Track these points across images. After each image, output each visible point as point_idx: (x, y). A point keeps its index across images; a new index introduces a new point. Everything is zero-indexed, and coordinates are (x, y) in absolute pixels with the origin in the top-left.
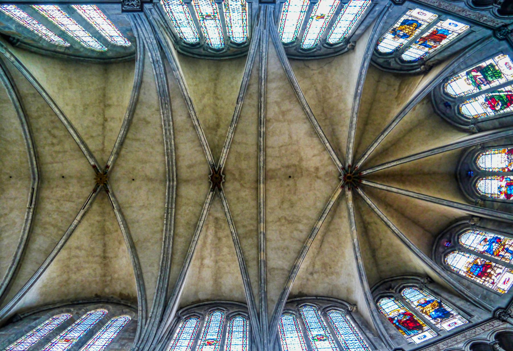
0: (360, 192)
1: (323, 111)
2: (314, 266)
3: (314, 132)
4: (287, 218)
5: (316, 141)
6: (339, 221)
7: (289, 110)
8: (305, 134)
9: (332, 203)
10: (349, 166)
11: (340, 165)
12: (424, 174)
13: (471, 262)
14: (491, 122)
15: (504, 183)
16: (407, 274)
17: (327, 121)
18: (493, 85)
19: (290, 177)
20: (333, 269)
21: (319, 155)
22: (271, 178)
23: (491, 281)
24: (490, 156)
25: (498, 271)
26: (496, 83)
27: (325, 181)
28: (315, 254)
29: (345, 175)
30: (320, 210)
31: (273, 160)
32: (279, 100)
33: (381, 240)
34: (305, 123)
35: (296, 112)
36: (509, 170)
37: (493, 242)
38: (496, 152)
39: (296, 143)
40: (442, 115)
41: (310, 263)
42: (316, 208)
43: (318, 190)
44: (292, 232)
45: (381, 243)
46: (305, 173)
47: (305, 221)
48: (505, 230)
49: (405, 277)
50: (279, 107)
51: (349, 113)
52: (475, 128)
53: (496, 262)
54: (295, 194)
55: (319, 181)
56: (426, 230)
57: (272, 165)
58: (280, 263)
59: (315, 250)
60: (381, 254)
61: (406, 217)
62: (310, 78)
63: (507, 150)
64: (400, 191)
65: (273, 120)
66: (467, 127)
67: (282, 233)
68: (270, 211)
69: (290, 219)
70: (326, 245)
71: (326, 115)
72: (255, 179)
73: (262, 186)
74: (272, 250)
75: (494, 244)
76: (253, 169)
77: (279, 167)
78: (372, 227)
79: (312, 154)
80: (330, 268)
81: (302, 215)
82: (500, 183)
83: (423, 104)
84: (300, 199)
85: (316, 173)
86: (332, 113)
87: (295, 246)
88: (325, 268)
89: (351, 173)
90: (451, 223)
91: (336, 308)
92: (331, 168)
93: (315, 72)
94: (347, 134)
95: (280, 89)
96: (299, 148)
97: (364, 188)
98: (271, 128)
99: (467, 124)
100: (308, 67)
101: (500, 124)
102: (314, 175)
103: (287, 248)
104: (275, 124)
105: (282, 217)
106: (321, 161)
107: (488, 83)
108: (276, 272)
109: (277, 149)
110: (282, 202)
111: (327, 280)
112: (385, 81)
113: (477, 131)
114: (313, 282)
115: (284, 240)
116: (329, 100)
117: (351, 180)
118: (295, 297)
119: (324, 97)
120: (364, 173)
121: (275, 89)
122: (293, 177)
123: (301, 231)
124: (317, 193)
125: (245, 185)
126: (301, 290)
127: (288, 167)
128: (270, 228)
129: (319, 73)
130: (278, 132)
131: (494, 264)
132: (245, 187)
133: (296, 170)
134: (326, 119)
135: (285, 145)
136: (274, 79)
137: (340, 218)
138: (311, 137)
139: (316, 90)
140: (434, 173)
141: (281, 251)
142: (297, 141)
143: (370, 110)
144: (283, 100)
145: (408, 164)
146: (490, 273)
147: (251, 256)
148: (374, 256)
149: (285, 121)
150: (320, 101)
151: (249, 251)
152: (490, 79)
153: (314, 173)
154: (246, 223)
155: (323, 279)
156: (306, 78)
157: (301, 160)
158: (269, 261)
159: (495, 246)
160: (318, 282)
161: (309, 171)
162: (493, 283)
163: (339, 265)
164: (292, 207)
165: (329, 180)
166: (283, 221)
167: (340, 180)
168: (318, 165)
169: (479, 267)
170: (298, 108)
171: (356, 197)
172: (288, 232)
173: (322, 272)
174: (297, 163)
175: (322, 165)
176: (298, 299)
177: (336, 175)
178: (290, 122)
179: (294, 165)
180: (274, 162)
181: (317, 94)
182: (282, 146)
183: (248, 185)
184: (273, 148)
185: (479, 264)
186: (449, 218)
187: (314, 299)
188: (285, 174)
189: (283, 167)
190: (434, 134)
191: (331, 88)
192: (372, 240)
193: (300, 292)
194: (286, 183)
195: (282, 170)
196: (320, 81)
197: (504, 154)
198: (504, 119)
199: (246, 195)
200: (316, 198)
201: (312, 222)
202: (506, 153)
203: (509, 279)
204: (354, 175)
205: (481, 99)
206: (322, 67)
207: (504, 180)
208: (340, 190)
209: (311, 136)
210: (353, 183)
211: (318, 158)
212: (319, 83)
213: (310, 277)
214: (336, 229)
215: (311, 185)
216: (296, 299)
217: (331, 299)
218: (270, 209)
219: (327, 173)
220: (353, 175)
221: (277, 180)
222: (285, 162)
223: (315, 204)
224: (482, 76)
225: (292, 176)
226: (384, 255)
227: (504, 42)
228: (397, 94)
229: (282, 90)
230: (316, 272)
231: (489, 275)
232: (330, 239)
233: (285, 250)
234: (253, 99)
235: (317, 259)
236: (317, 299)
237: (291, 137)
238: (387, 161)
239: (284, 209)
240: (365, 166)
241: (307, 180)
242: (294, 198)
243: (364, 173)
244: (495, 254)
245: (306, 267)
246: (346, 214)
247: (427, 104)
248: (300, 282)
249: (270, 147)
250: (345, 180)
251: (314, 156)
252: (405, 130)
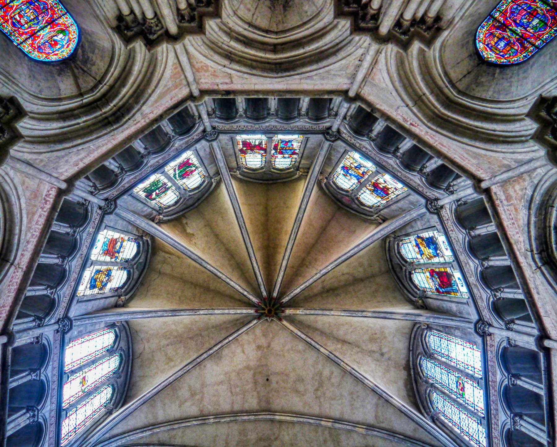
0: (285, 300)
1: (191, 338)
2: (374, 352)
3: (216, 356)
4: (315, 388)
5: (226, 352)
6: (320, 323)
7: (190, 387)
8: (217, 365)
9: (299, 333)
10: (256, 311)
11: (255, 322)
12: (267, 220)
16: (384, 245)
17: (203, 333)
19: (267, 380)
20: (377, 332)
21: (242, 346)
22: (268, 402)
27: (273, 338)
28: (359, 350)
29: (266, 316)
30: (307, 347)
31: (246, 401)
32: (177, 403)
33: (343, 274)
34: (205, 366)
35: (192, 380)
39: (228, 375)
40: (200, 202)
41: (369, 356)
42: (304, 351)
43: (284, 347)
44: (333, 385)
45: (347, 274)
46: (264, 362)
47: (320, 366)
49: (387, 249)
50: (186, 401)
51: (196, 318)
52: (216, 178)
54: (287, 375)
55: (273, 345)
56: (332, 219)
57: (253, 403)
58: (369, 407)
59: (354, 350)
60: (360, 273)
61: (316, 242)
62: (153, 352)
64: (286, 257)
65: (201, 406)
67: (333, 397)
68: (307, 408)
69: (316, 384)
70: (348, 338)
71: (197, 335)
72: (270, 422)
73: (277, 417)
74: (354, 413)
76: (258, 425)
77: (255, 393)
78: (328, 284)
79: (242, 354)
80: (376, 334)
81: (312, 369)
83: (187, 223)
84: (294, 369)
85: (264, 348)
86: (195, 329)
87: (349, 384)
88: (376, 339)
89: (264, 309)
90: (324, 193)
91: (424, 336)
92: (258, 331)
93: (146, 346)
94: (219, 316)
95: (164, 405)
96: (234, 371)
97: (282, 294)
98: (209, 407)
100: (141, 354)
101: (211, 163)
102: (265, 350)
103: (351, 393)
104: (205, 404)
105: (314, 394)
106: (249, 343)
108: (380, 414)
109: (234, 398)
110: (297, 392)
111: (390, 338)
112: (159, 266)
114: (392, 353)
115: (342, 396)
116: (180, 331)
117: (273, 309)
118: (411, 375)
119: (176, 337)
120: (265, 294)
121: (164, 410)
122: (269, 376)
123: (332, 373)
124: (286, 348)
125: (276, 435)
126: (402, 368)
127: (256, 383)
128: (327, 410)
129: (148, 342)
130: (214, 399)
132: (279, 435)
133: (260, 372)
134: (201, 335)
135: (231, 388)
136: (153, 413)
137: (317, 322)
138: (221, 357)
139: (168, 345)
140: (266, 208)
141: (355, 403)
142: (226, 374)
143: (192, 283)
144: (178, 398)
145: (255, 243)
147: (361, 441)
148: (362, 280)
149: (202, 392)
150: (181, 342)
151: (354, 441)
153: (263, 350)
154: (321, 439)
155: (389, 342)
156: (153, 356)
157: (248, 368)
158: (366, 419)
160: (393, 348)
161: (261, 357)
163: (372, 325)
164: (303, 380)
165: (272, 332)
166: (319, 393)
167: (272, 320)
168: (254, 346)
170: (187, 378)
171: (294, 303)
172: (333, 389)
173: (381, 342)
174: (252, 372)
175: (254, 341)
176: (412, 373)
177: (267, 324)
178: (203, 385)
179: (254, 375)
180: (250, 400)
181: (172, 345)
182: (232, 393)
183: (276, 430)
184: (233, 403)
186: (319, 196)
187: (413, 354)
188: (264, 385)
189: (256, 388)
190: (221, 213)
191: (166, 330)
192: (342, 283)
193: (405, 368)
194: (274, 385)
195: (259, 389)
196: (157, 341)
199: (288, 435)
200: (292, 350)
201: (321, 358)
204: (266, 306)
206: (142, 340)
208: (285, 322)
209: (220, 358)
210: (276, 307)
211: (246, 346)
212: (160, 342)
213: (386, 356)
214: (330, 326)
215: (277, 355)
216: (413, 376)
217: (413, 336)
218: (304, 407)
219: (264, 335)
220: (267, 307)
221: (271, 395)
222: (249, 386)
223: (299, 352)
225: (266, 378)
226: (361, 269)
227: (118, 202)
228: (174, 256)
229: (167, 401)
230: (380, 349)
232: (341, 333)
233: (355, 397)
234: (175, 435)
235: (364, 348)
236: (412, 350)
237: (221, 383)
238: (251, 267)
239: (306, 390)
240: (258, 294)
241: (272, 359)
242: (293, 376)
243: (265, 294)
245: (375, 362)
246: (312, 318)
247: (187, 219)
248: (392, 369)
249: (233, 407)
250: (273, 316)
251: (243, 352)
252: (216, 243)
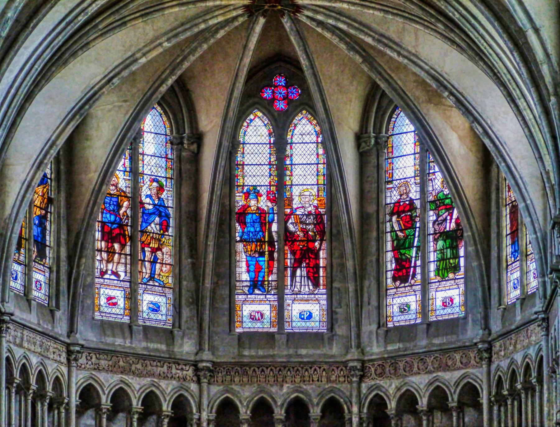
13: (120, 186)
14: (374, 196)
15: (264, 204)
18: (431, 246)
23: (103, 266)
24: (313, 159)
25: (121, 269)
26: (432, 257)
36: (288, 217)
37: (160, 216)
38: (321, 182)
48: (184, 239)
53: (133, 255)
63: (322, 211)
66: (371, 129)
75: (157, 220)
82: (263, 190)
99: (377, 130)
107: (435, 234)
113: (361, 150)
131: (128, 250)
146: (114, 253)
152: (440, 243)
159: (154, 228)
162: (103, 273)
169: (116, 216)
185: (121, 212)
197: (316, 203)
198: (374, 234)
202: (316, 208)
203: (115, 304)
205: (414, 194)
207: (269, 204)
224: (448, 229)
231: (111, 252)
244: (144, 238)
